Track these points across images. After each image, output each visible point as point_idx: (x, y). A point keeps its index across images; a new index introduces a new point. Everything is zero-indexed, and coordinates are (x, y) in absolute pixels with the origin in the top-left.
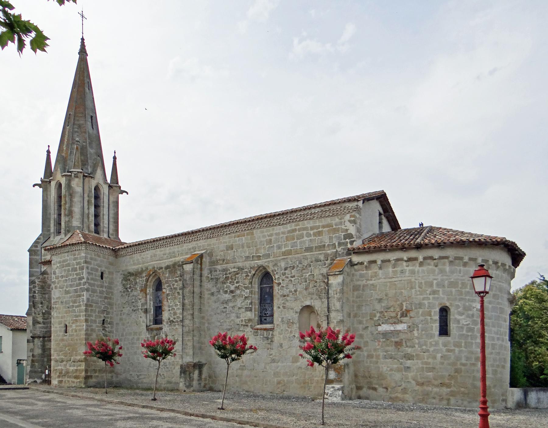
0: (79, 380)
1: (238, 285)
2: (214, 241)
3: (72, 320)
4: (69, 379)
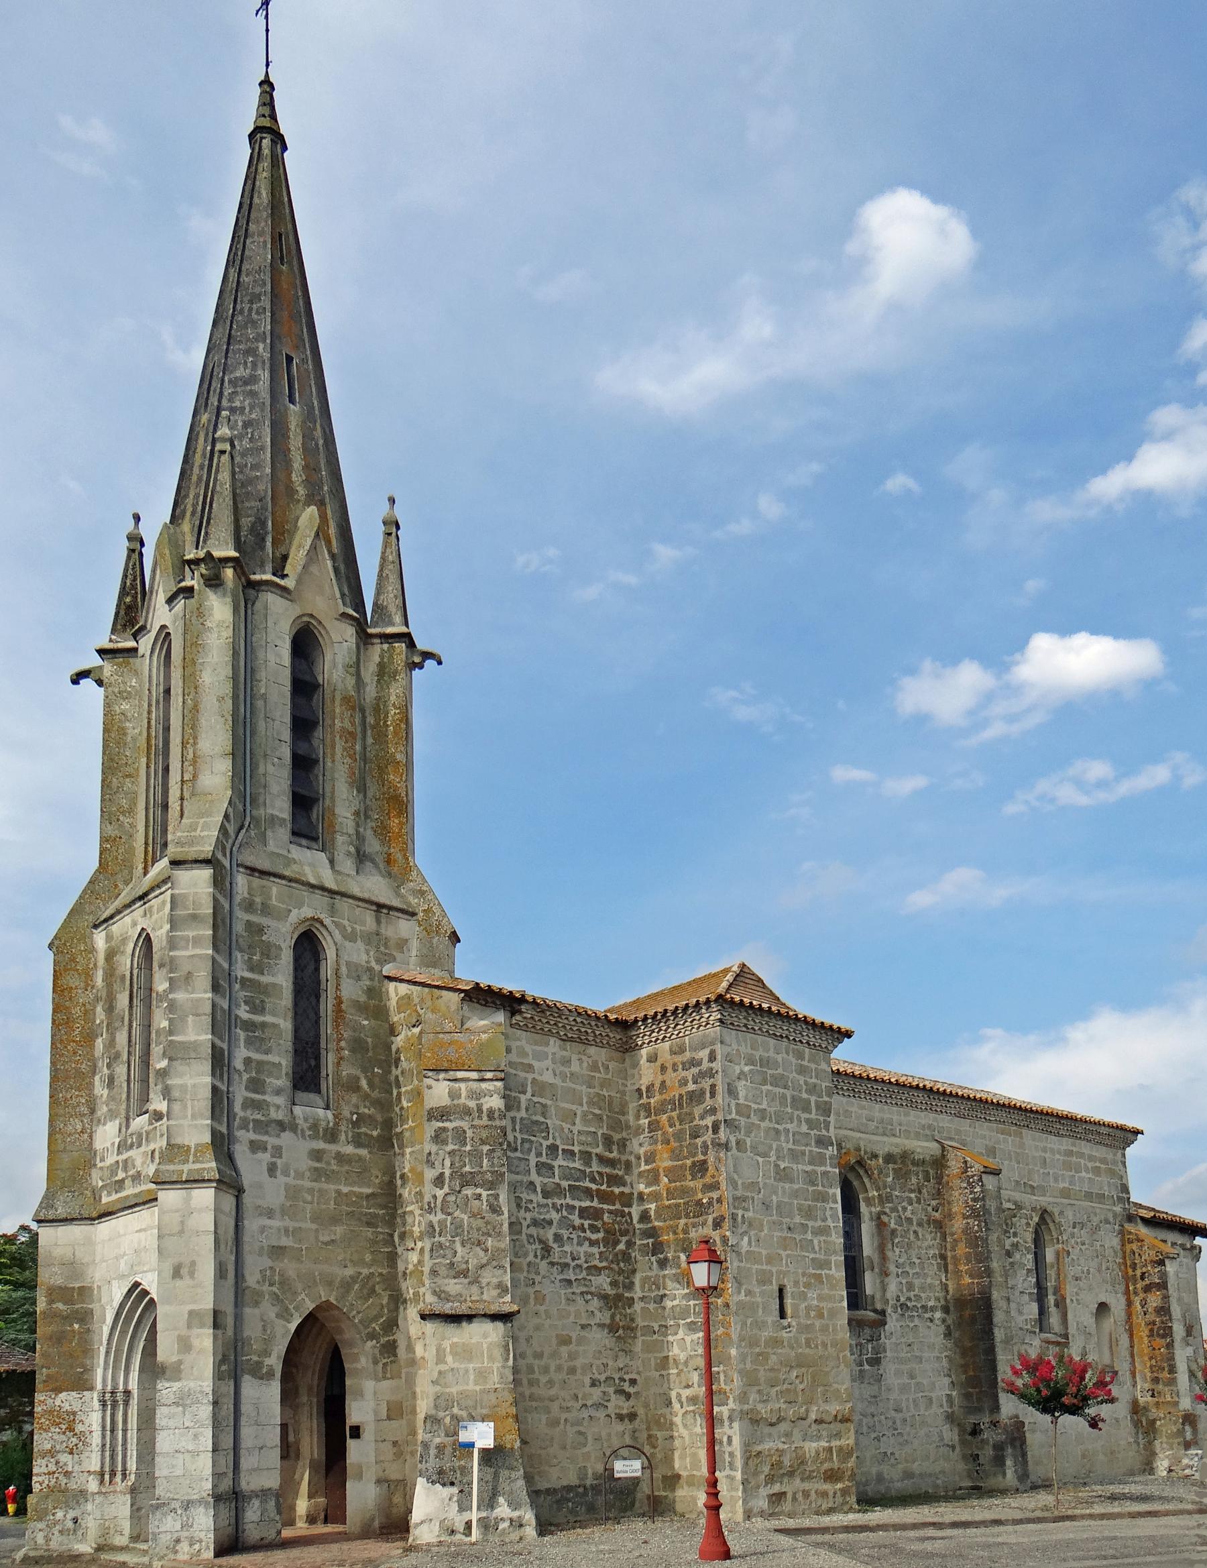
0: (839, 1486)
1: (1015, 1240)
2: (965, 1125)
3: (804, 1274)
4: (807, 1486)
